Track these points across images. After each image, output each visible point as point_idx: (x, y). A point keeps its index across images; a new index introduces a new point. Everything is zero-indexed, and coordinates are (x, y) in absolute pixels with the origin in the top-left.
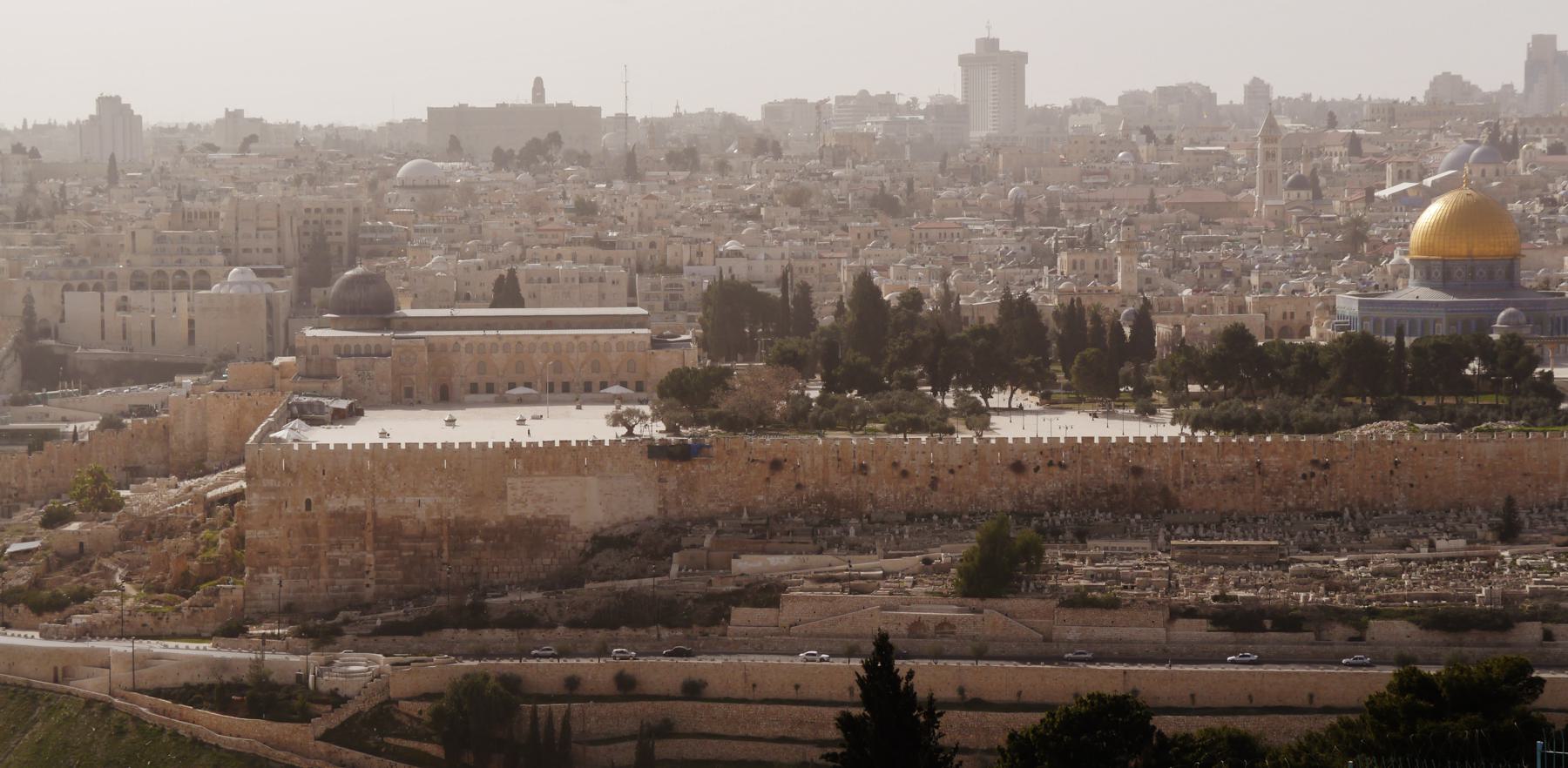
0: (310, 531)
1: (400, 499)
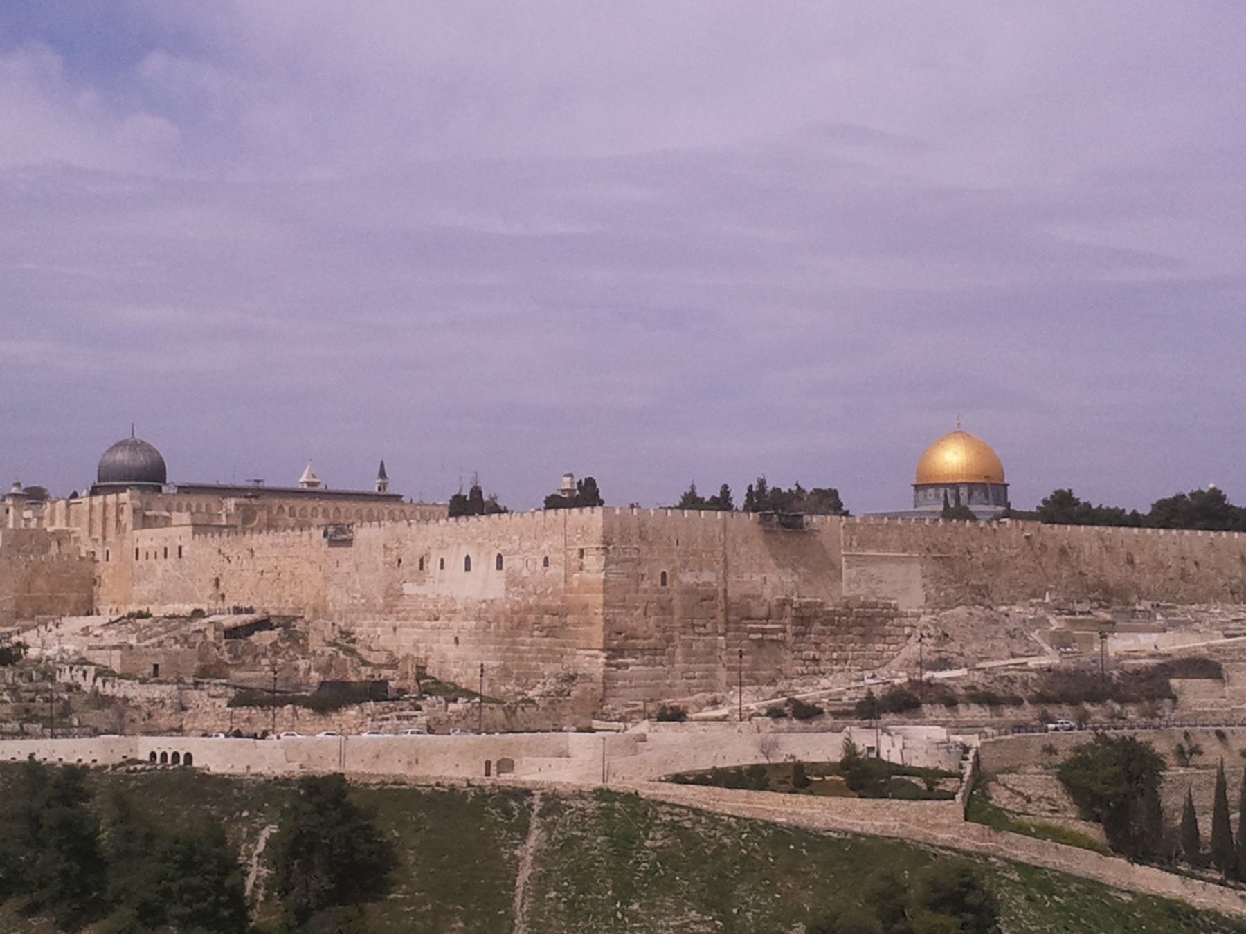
0: (665, 608)
1: (746, 576)
